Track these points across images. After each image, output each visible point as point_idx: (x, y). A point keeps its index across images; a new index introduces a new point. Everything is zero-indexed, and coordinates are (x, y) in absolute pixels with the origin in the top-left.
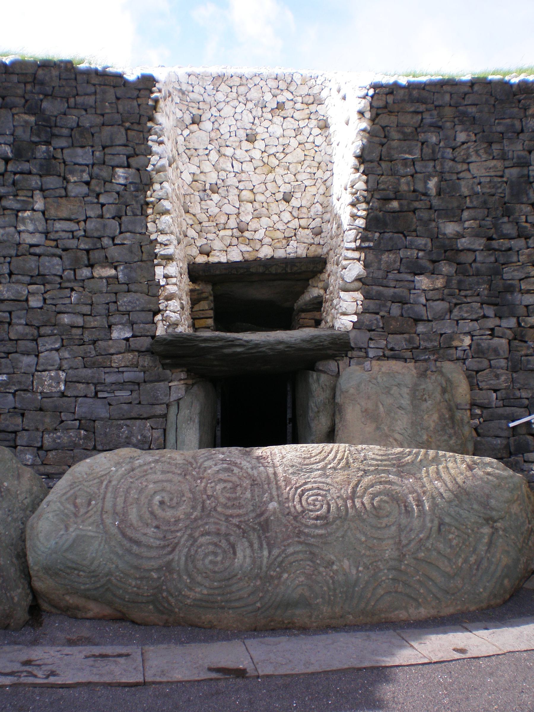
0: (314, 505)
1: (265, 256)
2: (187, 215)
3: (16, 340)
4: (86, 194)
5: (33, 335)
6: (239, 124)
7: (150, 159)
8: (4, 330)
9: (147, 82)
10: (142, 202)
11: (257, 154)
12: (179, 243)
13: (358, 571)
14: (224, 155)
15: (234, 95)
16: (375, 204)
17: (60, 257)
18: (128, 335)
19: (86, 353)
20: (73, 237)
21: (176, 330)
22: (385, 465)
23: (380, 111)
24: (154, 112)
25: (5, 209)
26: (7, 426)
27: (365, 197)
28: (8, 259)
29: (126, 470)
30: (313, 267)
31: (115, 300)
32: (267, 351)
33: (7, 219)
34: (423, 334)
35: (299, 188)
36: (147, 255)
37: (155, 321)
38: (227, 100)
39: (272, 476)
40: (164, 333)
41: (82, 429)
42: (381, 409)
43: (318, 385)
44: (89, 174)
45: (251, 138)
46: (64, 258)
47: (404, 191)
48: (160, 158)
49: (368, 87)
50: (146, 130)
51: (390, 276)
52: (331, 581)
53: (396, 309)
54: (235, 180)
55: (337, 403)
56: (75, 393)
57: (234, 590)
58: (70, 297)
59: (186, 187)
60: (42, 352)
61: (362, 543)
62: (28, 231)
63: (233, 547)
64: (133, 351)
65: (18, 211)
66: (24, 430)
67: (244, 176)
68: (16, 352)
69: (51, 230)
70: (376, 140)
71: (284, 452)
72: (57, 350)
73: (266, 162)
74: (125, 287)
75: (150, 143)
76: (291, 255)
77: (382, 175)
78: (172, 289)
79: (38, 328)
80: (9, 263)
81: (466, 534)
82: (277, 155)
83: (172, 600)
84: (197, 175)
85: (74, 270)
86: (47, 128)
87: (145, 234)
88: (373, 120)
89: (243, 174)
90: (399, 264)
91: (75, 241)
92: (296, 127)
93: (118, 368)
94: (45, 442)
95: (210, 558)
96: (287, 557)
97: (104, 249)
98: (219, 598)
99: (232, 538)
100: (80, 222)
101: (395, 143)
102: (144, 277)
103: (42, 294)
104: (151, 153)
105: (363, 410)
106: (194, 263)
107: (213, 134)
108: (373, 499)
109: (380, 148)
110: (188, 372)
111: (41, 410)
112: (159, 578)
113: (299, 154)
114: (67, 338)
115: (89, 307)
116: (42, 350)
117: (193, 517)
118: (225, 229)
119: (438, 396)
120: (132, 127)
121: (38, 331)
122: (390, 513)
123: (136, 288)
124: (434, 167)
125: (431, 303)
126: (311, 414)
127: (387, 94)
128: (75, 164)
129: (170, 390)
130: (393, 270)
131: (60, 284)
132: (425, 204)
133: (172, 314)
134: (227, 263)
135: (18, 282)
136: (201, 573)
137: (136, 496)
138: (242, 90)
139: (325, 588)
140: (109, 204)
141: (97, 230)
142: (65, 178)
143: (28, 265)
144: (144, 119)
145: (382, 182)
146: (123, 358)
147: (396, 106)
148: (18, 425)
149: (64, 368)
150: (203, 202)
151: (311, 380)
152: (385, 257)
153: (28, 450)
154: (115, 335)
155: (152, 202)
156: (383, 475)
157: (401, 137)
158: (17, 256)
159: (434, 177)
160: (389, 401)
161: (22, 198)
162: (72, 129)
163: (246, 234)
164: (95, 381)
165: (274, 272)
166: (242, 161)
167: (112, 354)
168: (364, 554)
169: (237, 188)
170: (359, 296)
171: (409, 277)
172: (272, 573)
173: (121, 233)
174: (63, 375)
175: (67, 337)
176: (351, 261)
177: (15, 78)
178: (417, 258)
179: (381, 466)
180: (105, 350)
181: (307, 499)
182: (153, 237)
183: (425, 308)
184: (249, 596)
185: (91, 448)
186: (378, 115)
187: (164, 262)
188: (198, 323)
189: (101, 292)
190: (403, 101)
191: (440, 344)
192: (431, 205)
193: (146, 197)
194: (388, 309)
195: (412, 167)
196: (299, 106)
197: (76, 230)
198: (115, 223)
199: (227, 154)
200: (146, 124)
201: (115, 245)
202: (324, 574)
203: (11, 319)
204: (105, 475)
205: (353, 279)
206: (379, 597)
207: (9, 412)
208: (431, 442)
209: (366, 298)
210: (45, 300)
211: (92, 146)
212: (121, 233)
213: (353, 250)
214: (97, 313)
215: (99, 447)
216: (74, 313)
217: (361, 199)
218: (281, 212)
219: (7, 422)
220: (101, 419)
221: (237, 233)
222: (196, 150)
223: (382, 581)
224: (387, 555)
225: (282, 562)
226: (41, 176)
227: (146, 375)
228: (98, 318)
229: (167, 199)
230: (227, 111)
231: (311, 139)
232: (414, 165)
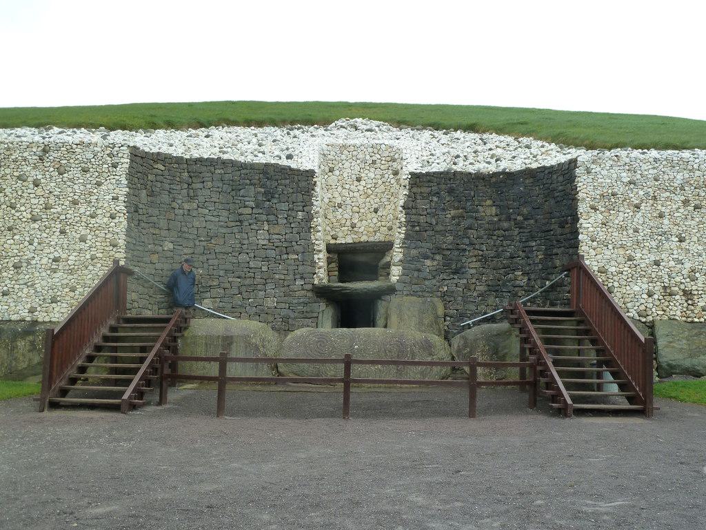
11: (361, 188)
16: (409, 227)
30: (387, 247)
36: (309, 250)
43: (381, 307)
45: (359, 180)
53: (416, 274)
78: (321, 264)
86: (269, 195)
138: (355, 153)
174: (275, 299)
196: (383, 162)
209: (403, 269)
230: (347, 164)
231: (389, 180)
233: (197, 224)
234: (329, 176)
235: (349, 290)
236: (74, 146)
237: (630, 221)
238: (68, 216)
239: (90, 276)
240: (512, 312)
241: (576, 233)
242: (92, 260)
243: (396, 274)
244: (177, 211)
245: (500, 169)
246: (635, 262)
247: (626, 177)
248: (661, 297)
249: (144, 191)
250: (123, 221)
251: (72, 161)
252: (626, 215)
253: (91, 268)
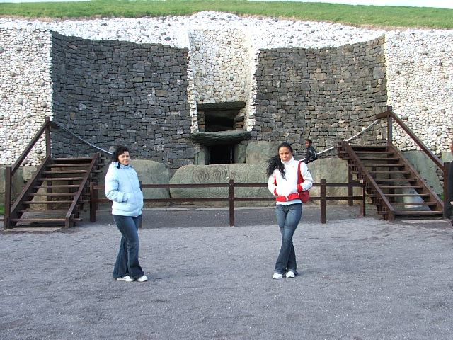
36: (187, 105)
43: (240, 148)
67: (215, 71)
101: (266, 70)
113: (236, 62)
114: (165, 134)
170: (254, 120)
188: (201, 126)
196: (236, 43)
230: (209, 45)
233: (102, 90)
236: (9, 32)
237: (423, 82)
238: (8, 85)
239: (27, 130)
240: (340, 149)
241: (384, 91)
242: (28, 118)
244: (87, 81)
245: (326, 46)
246: (427, 111)
247: (420, 49)
248: (446, 136)
249: (64, 66)
250: (48, 91)
251: (8, 43)
252: (421, 77)
253: (27, 123)
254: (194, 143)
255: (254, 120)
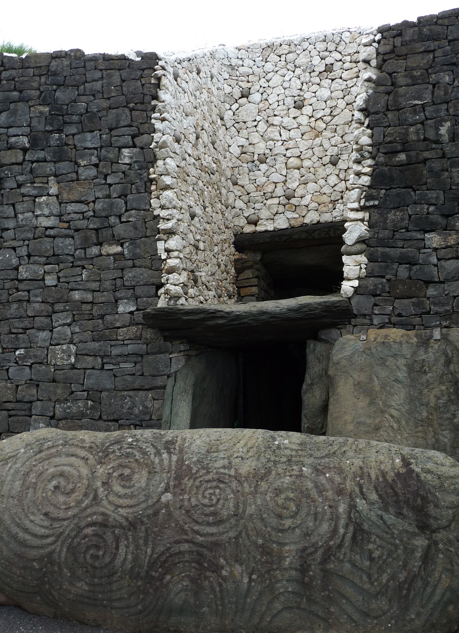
0: (211, 500)
1: (311, 221)
2: (236, 187)
3: (34, 317)
4: (94, 176)
5: (47, 312)
6: (287, 92)
7: (153, 136)
8: (22, 307)
9: (150, 60)
10: (146, 179)
11: (304, 120)
12: (193, 216)
13: (251, 580)
14: (273, 125)
15: (283, 63)
16: (381, 159)
17: (73, 237)
18: (133, 309)
19: (94, 327)
20: (84, 218)
21: (177, 303)
22: (300, 456)
23: (386, 57)
24: (158, 90)
25: (24, 195)
26: (24, 397)
27: (370, 153)
28: (26, 242)
29: (33, 452)
31: (120, 275)
32: (250, 322)
33: (25, 205)
34: (433, 297)
35: (346, 150)
36: (150, 229)
37: (159, 294)
38: (275, 70)
39: (173, 463)
40: (166, 306)
41: (90, 400)
42: (376, 382)
44: (97, 156)
46: (75, 237)
47: (413, 141)
48: (164, 135)
49: (375, 32)
50: (150, 108)
51: (397, 236)
52: (218, 589)
53: (403, 271)
54: (283, 148)
55: (328, 377)
56: (84, 366)
57: (114, 589)
58: (81, 275)
59: (234, 160)
60: (56, 328)
61: (257, 546)
62: (44, 215)
63: (117, 540)
64: (137, 324)
65: (36, 197)
66: (38, 400)
68: (33, 328)
69: (64, 213)
70: (382, 88)
71: (196, 437)
72: (69, 325)
73: (313, 127)
74: (130, 263)
75: (153, 121)
76: (338, 218)
77: (389, 126)
78: (172, 262)
79: (53, 304)
80: (28, 245)
81: (392, 544)
82: (324, 118)
83: (55, 594)
84: (246, 147)
85: (85, 249)
86: (59, 116)
87: (149, 209)
88: (379, 67)
89: (290, 142)
90: (407, 222)
91: (85, 222)
92: (344, 87)
93: (123, 341)
94: (57, 411)
95: (91, 552)
96: (171, 556)
97: (112, 227)
98: (100, 596)
99: (116, 532)
100: (89, 203)
101: (401, 90)
102: (147, 252)
103: (57, 273)
104: (154, 131)
105: (356, 383)
106: (241, 233)
107: (261, 105)
108: (277, 495)
109: (386, 98)
110: (189, 342)
111: (54, 381)
112: (41, 569)
114: (78, 313)
115: (98, 284)
116: (56, 325)
117: (83, 505)
118: (272, 197)
119: (440, 368)
120: (135, 108)
121: (53, 308)
122: (296, 513)
123: (140, 263)
124: (447, 110)
125: (443, 262)
126: (304, 387)
127: (394, 37)
128: (85, 148)
129: (171, 362)
130: (401, 229)
131: (72, 262)
132: (437, 153)
133: (172, 288)
134: (274, 231)
135: (35, 263)
136: (82, 568)
137: (34, 481)
138: (291, 57)
139: (211, 596)
140: (116, 184)
141: (104, 210)
142: (76, 163)
143: (43, 247)
144: (148, 98)
145: (389, 134)
146: (127, 331)
147: (404, 48)
148: (33, 396)
149: (75, 342)
150: (251, 173)
151: (308, 350)
152: (391, 216)
153: (41, 419)
154: (121, 309)
155: (154, 178)
156: (295, 467)
157: (410, 81)
158: (34, 238)
159: (446, 121)
160: (383, 374)
161: (39, 185)
162: (82, 116)
163: (293, 201)
164: (102, 354)
165: (317, 237)
166: (289, 128)
167: (119, 328)
168: (260, 560)
169: (285, 156)
170: (363, 259)
171: (419, 236)
172: (153, 573)
173: (127, 211)
174: (73, 348)
175: (78, 312)
176: (354, 223)
177: (31, 71)
178: (428, 213)
179: (296, 456)
180: (111, 323)
181: (205, 491)
182: (156, 213)
183: (436, 269)
184: (130, 596)
185: (97, 418)
186: (384, 61)
187: (165, 237)
188: (244, 292)
189: (109, 269)
190: (412, 41)
191: (453, 307)
192: (444, 153)
193: (149, 174)
194: (394, 272)
195: (422, 114)
196: (347, 65)
197: (86, 212)
198: (121, 202)
199: (275, 123)
200: (150, 103)
201: (122, 222)
202: (211, 579)
203: (29, 298)
204: (13, 457)
205: (354, 241)
206: (276, 612)
207: (26, 383)
208: (432, 420)
209: (370, 260)
210: (59, 278)
211: (100, 130)
212: (127, 211)
213: (357, 210)
214: (105, 289)
215: (104, 417)
216: (84, 290)
217: (366, 154)
218: (328, 176)
219: (24, 393)
220: (107, 390)
221: (283, 200)
222: (245, 122)
223: (280, 594)
224: (287, 563)
225: (165, 561)
226: (55, 162)
227: (149, 347)
228: (105, 293)
229: (168, 174)
230: (276, 80)
232: (424, 111)
234: (240, 106)
235: (222, 317)
243: (351, 275)
254: (166, 339)
255: (363, 259)
